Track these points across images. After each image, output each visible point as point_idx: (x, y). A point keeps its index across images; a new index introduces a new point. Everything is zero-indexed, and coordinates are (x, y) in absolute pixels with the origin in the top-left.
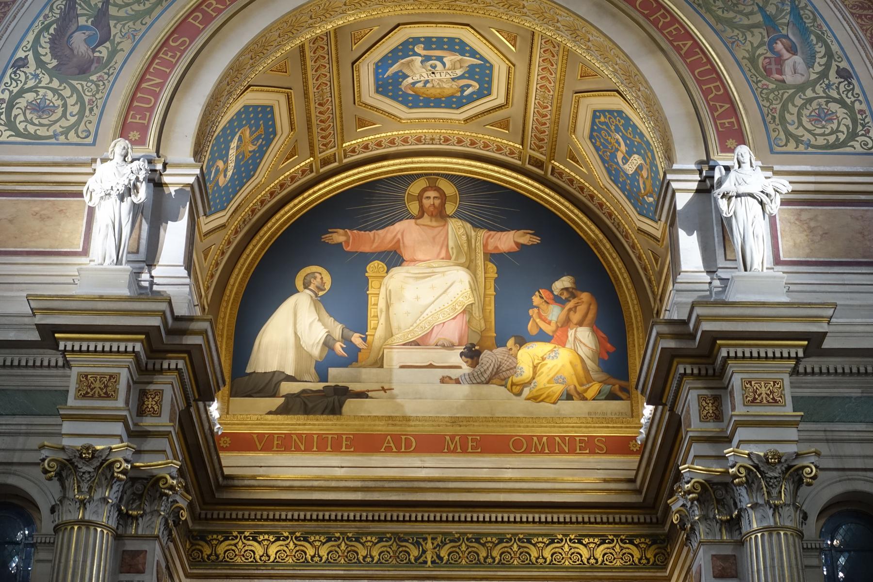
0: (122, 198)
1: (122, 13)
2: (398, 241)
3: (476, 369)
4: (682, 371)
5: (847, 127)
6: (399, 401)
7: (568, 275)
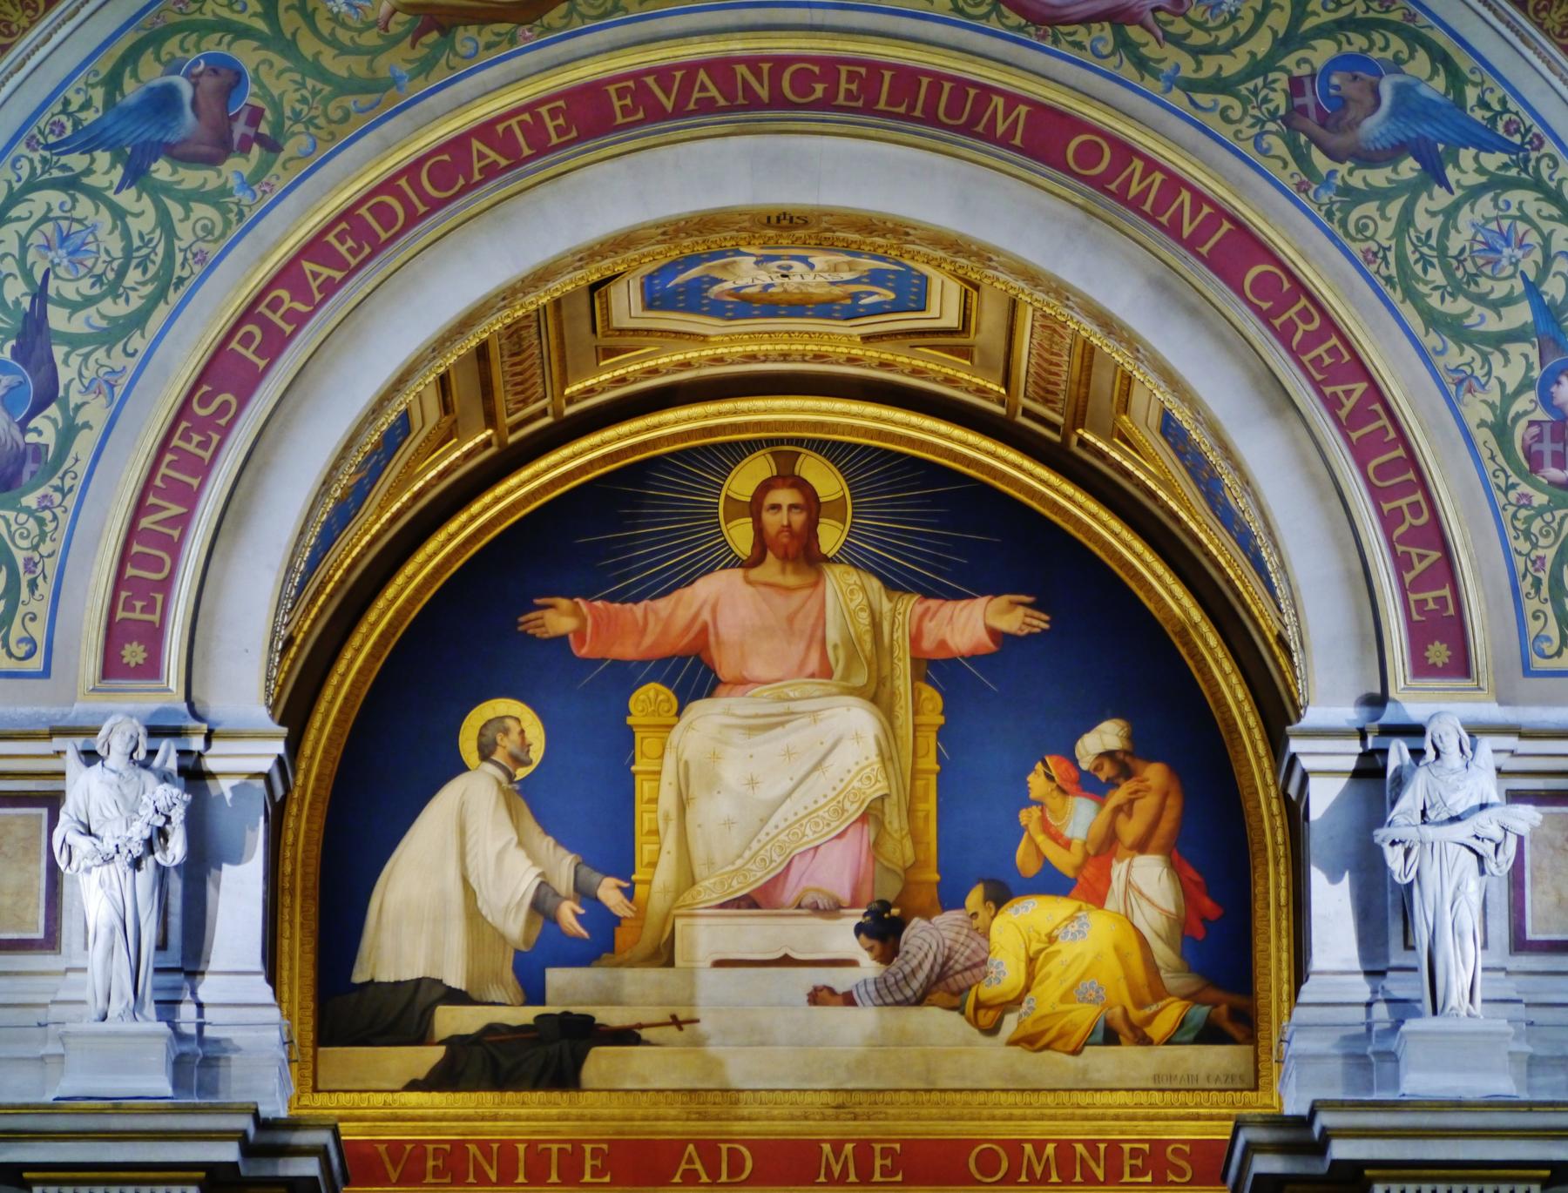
0: (136, 864)
1: (78, 325)
2: (704, 630)
3: (893, 969)
6: (712, 1050)
7: (1114, 716)
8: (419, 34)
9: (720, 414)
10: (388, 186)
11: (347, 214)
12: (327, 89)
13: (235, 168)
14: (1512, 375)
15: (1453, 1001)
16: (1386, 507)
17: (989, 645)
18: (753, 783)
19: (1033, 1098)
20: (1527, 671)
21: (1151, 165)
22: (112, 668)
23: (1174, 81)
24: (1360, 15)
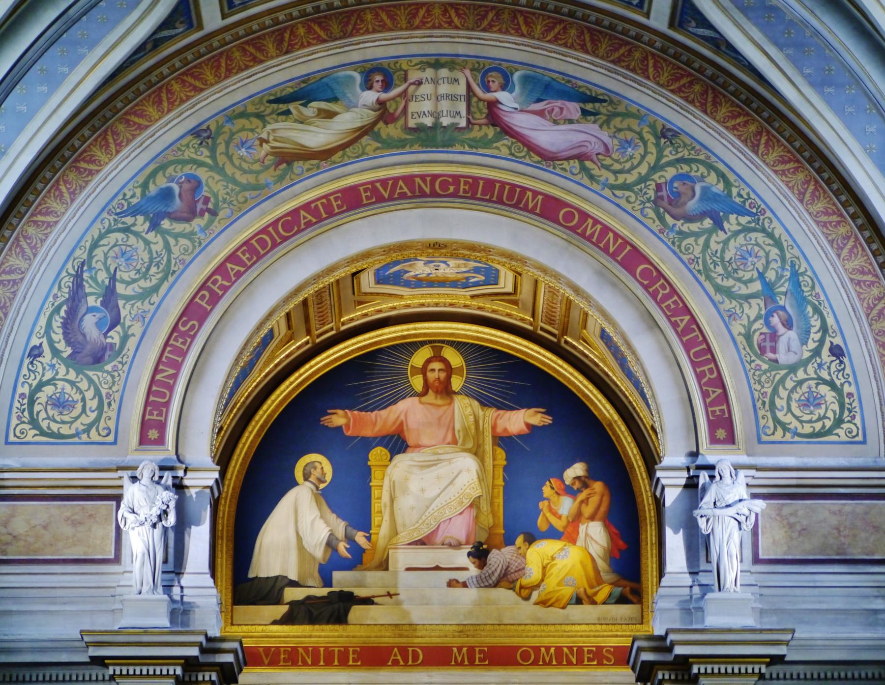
0: (154, 526)
1: (129, 291)
2: (402, 424)
3: (484, 571)
4: (660, 677)
5: (834, 412)
6: (405, 607)
7: (580, 461)
8: (277, 165)
9: (408, 330)
10: (264, 231)
11: (246, 243)
12: (238, 189)
13: (198, 223)
14: (753, 313)
15: (728, 585)
16: (698, 370)
17: (526, 431)
18: (423, 490)
19: (545, 628)
20: (760, 441)
21: (596, 222)
22: (144, 440)
23: (606, 185)
24: (686, 157)
